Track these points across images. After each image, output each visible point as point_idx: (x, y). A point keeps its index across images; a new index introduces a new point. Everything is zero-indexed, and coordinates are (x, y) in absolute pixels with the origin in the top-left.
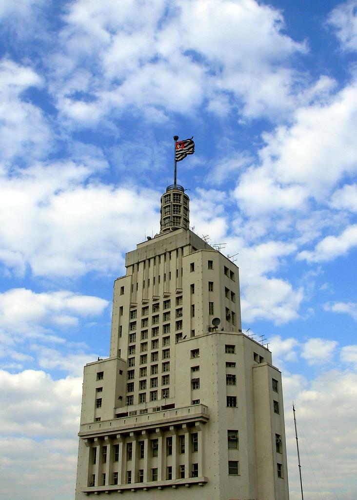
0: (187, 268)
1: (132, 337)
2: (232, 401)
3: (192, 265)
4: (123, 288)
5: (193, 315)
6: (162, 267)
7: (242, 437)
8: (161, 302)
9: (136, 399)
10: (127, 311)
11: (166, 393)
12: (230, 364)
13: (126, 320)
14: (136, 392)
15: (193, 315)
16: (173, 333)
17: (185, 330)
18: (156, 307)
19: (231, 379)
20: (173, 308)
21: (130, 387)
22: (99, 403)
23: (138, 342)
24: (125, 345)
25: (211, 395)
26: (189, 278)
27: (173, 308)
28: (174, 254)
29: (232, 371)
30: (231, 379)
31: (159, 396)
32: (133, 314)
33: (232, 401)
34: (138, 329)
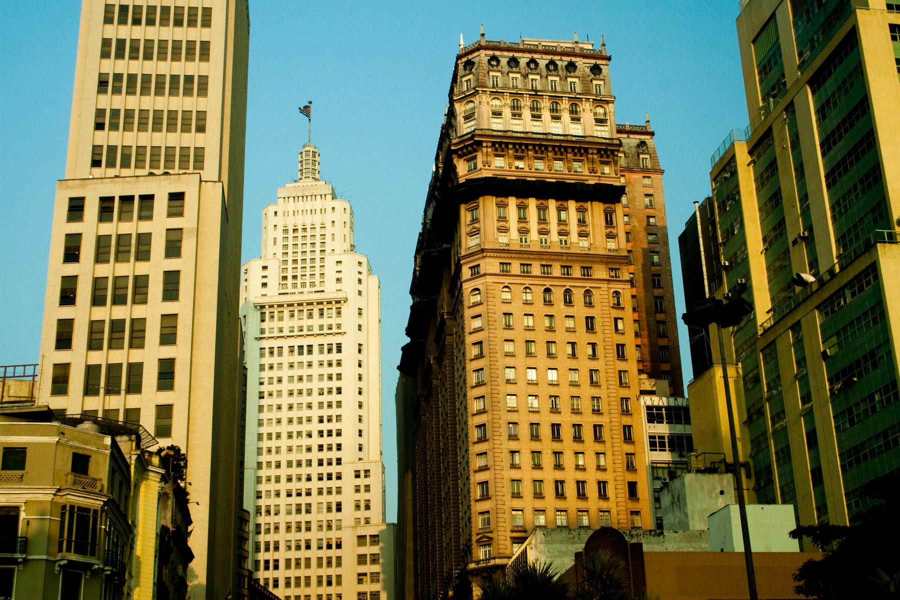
0: (329, 210)
1: (285, 246)
2: (360, 293)
3: (333, 208)
4: (276, 213)
5: (333, 239)
6: (309, 205)
7: (364, 312)
8: (308, 227)
9: (290, 286)
10: (280, 228)
11: (312, 284)
12: (360, 273)
13: (279, 234)
14: (290, 281)
15: (333, 239)
16: (318, 248)
17: (328, 249)
18: (305, 230)
19: (360, 281)
20: (318, 232)
21: (285, 278)
22: (264, 285)
23: (290, 250)
24: (279, 250)
25: (349, 287)
26: (329, 217)
27: (318, 232)
28: (318, 197)
29: (360, 277)
30: (360, 281)
31: (308, 285)
32: (286, 231)
33: (360, 293)
34: (290, 242)
